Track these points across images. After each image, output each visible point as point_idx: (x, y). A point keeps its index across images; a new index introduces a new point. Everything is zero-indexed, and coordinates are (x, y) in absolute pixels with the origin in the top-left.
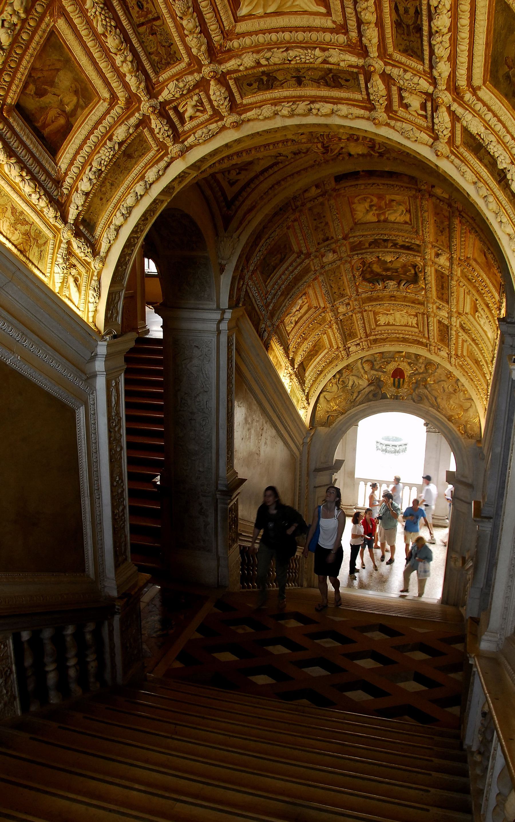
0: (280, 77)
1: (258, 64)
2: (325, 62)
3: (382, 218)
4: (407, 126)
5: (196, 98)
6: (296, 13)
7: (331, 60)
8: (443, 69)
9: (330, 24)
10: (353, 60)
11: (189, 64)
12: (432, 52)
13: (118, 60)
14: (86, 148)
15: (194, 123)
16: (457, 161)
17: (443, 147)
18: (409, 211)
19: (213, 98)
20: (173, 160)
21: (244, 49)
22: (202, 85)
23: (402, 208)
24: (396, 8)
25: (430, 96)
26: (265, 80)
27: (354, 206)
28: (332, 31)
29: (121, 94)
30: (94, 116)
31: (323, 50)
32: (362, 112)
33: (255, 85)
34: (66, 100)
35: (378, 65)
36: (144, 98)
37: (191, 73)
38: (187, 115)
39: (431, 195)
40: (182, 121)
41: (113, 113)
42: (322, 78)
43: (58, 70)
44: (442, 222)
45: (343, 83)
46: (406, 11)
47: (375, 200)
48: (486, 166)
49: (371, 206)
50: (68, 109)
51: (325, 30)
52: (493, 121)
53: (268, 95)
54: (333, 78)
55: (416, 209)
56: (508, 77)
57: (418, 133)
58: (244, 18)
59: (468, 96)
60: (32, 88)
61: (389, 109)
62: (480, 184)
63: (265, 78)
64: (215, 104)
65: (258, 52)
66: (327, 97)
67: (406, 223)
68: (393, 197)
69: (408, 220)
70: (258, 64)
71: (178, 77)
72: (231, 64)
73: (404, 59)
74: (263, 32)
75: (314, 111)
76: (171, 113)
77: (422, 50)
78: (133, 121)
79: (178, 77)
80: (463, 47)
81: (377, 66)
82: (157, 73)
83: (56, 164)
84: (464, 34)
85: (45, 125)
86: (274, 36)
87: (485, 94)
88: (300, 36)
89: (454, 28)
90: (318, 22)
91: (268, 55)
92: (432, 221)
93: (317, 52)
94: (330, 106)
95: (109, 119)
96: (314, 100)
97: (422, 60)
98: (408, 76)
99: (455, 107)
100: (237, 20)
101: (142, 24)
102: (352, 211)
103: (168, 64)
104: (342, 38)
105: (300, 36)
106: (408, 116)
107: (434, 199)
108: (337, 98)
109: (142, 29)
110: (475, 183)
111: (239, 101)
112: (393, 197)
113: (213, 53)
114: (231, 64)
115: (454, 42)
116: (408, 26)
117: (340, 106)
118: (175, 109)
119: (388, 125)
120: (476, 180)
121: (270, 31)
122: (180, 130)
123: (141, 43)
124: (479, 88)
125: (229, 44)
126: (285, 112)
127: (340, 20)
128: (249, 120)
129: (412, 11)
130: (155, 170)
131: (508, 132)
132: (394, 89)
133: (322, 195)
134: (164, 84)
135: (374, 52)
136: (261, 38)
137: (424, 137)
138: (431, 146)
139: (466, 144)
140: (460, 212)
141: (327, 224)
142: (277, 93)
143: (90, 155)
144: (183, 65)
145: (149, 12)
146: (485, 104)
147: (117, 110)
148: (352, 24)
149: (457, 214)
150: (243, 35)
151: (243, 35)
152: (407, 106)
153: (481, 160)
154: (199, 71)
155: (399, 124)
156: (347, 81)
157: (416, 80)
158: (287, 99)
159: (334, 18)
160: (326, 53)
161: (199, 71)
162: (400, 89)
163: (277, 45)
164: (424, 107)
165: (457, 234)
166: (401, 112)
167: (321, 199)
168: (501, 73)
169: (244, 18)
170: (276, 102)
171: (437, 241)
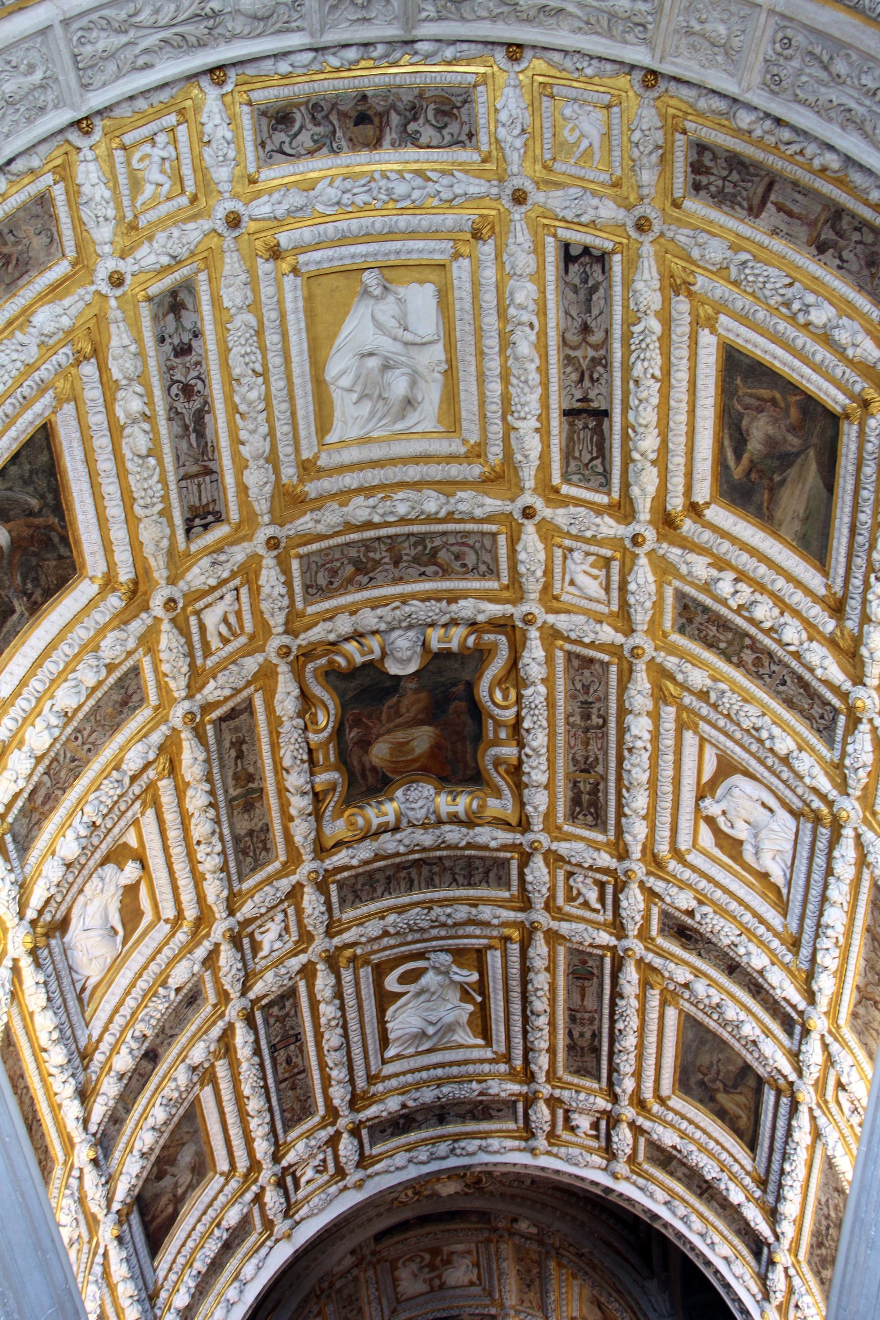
0: (420, 1118)
1: (404, 1106)
2: (481, 1094)
3: (437, 1282)
4: (574, 1151)
5: (321, 1156)
6: (451, 1048)
7: (491, 1091)
8: (629, 1084)
9: (489, 1054)
10: (515, 1088)
11: (323, 1118)
12: (613, 1069)
13: (253, 1123)
14: (190, 1244)
15: (310, 1188)
16: (641, 1181)
17: (622, 1168)
18: (477, 1265)
19: (341, 1153)
20: (277, 1241)
21: (388, 1092)
22: (333, 1141)
23: (467, 1261)
24: (570, 1034)
25: (607, 1114)
26: (402, 1123)
27: (397, 1273)
28: (491, 1061)
29: (242, 1164)
30: (206, 1199)
31: (480, 1082)
32: (516, 1143)
33: (389, 1131)
34: (181, 1181)
35: (546, 1090)
36: (267, 1164)
37: (324, 1127)
38: (303, 1180)
39: (512, 1234)
40: (297, 1187)
41: (228, 1189)
42: (470, 1111)
43: (183, 1144)
44: (529, 1271)
45: (494, 1113)
46: (582, 1035)
47: (427, 1257)
48: (679, 1180)
49: (421, 1269)
50: (180, 1191)
51: (482, 1061)
52: (691, 1129)
53: (403, 1140)
54: (483, 1109)
55: (489, 1260)
56: (702, 1083)
57: (588, 1157)
58: (392, 1060)
59: (656, 1108)
60: (155, 1170)
61: (551, 1135)
62: (676, 1203)
63: (402, 1121)
64: (343, 1160)
65: (403, 1094)
66: (474, 1133)
67: (472, 1284)
68: (454, 1248)
69: (474, 1278)
70: (404, 1106)
71: (309, 1134)
72: (372, 1111)
73: (576, 1080)
74: (412, 1071)
75: (458, 1151)
76: (289, 1179)
77: (599, 1069)
78: (249, 1196)
79: (309, 1134)
80: (650, 1063)
81: (545, 1091)
82: (285, 1132)
83: (155, 1271)
84: (652, 1050)
85: (154, 1218)
86: (424, 1075)
87: (676, 1103)
88: (455, 1070)
89: (641, 1046)
90: (476, 1054)
91: (418, 1094)
92: (514, 1272)
93: (474, 1085)
94: (477, 1142)
95: (222, 1198)
96: (457, 1138)
97: (599, 1079)
98: (582, 1096)
99: (640, 1121)
100: (384, 1062)
101: (285, 1080)
102: (395, 1281)
103: (300, 1120)
104: (503, 1068)
105: (455, 1070)
106: (574, 1139)
107: (517, 1239)
108: (485, 1132)
109: (283, 1085)
110: (666, 1203)
111: (367, 1153)
112: (454, 1248)
113: (356, 1102)
114: (372, 1111)
115: (640, 1058)
116: (582, 1048)
117: (490, 1141)
118: (293, 1174)
119: (549, 1153)
120: (668, 1198)
121: (419, 1070)
122: (293, 1200)
123: (279, 1100)
124: (669, 1098)
125: (373, 1089)
126: (423, 1157)
127: (503, 1049)
128: (377, 1174)
129: (588, 1035)
130: (254, 1261)
131: (710, 1137)
132: (560, 1113)
133: (357, 1266)
134: (289, 1146)
135: (541, 1077)
136: (409, 1078)
137: (597, 1160)
138: (605, 1169)
139: (650, 1159)
140: (557, 1249)
141: (360, 1310)
142: (413, 1137)
143: (193, 1251)
144: (316, 1119)
145: (296, 1066)
146: (676, 1113)
147: (233, 1184)
148: (518, 1052)
149: (553, 1252)
150: (389, 1077)
151: (389, 1077)
152: (573, 1129)
153: (671, 1174)
154: (333, 1124)
155: (563, 1150)
156: (499, 1110)
157: (592, 1099)
158: (424, 1141)
159: (495, 1048)
160: (484, 1085)
161: (333, 1124)
162: (567, 1111)
163: (426, 1083)
164: (595, 1126)
165: (554, 1283)
166: (566, 1136)
167: (355, 1272)
168: (693, 1081)
169: (392, 1060)
170: (410, 1148)
171: (523, 1301)
